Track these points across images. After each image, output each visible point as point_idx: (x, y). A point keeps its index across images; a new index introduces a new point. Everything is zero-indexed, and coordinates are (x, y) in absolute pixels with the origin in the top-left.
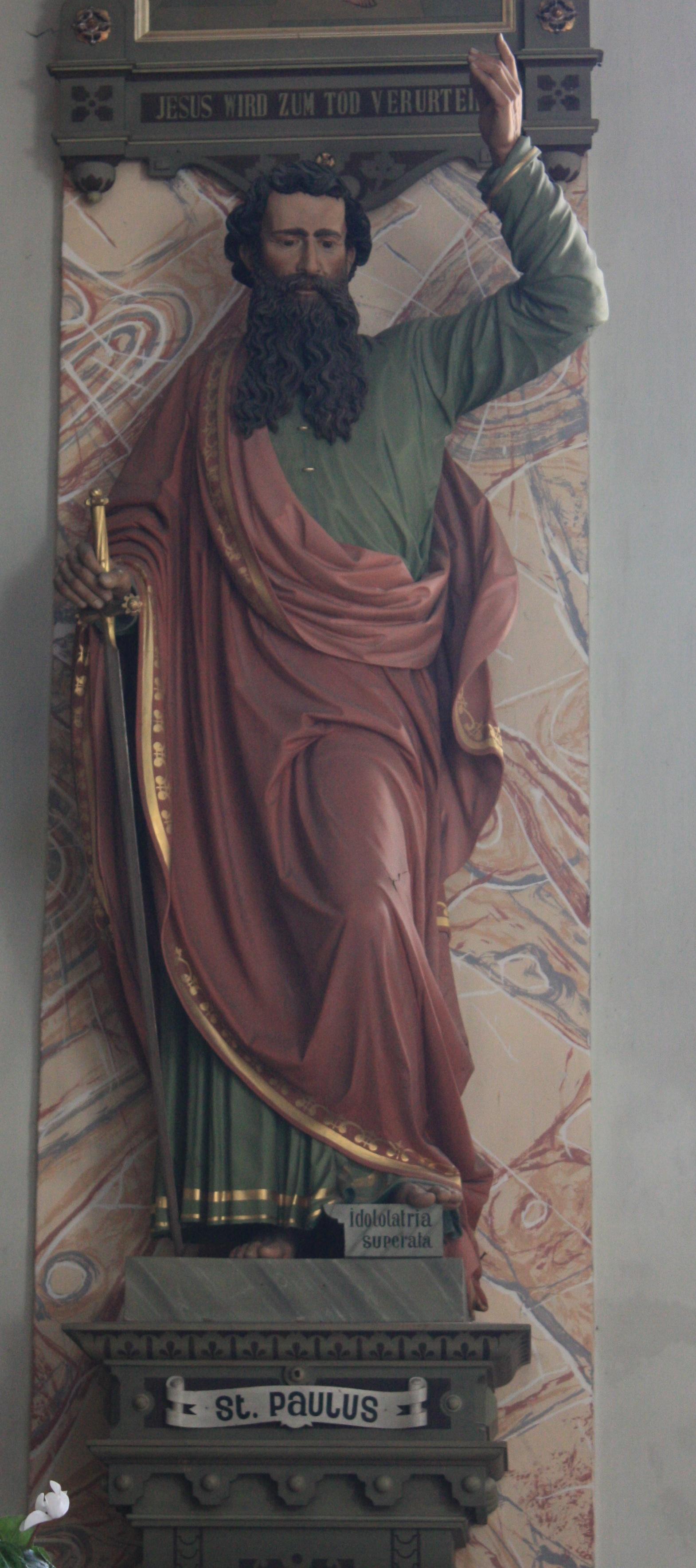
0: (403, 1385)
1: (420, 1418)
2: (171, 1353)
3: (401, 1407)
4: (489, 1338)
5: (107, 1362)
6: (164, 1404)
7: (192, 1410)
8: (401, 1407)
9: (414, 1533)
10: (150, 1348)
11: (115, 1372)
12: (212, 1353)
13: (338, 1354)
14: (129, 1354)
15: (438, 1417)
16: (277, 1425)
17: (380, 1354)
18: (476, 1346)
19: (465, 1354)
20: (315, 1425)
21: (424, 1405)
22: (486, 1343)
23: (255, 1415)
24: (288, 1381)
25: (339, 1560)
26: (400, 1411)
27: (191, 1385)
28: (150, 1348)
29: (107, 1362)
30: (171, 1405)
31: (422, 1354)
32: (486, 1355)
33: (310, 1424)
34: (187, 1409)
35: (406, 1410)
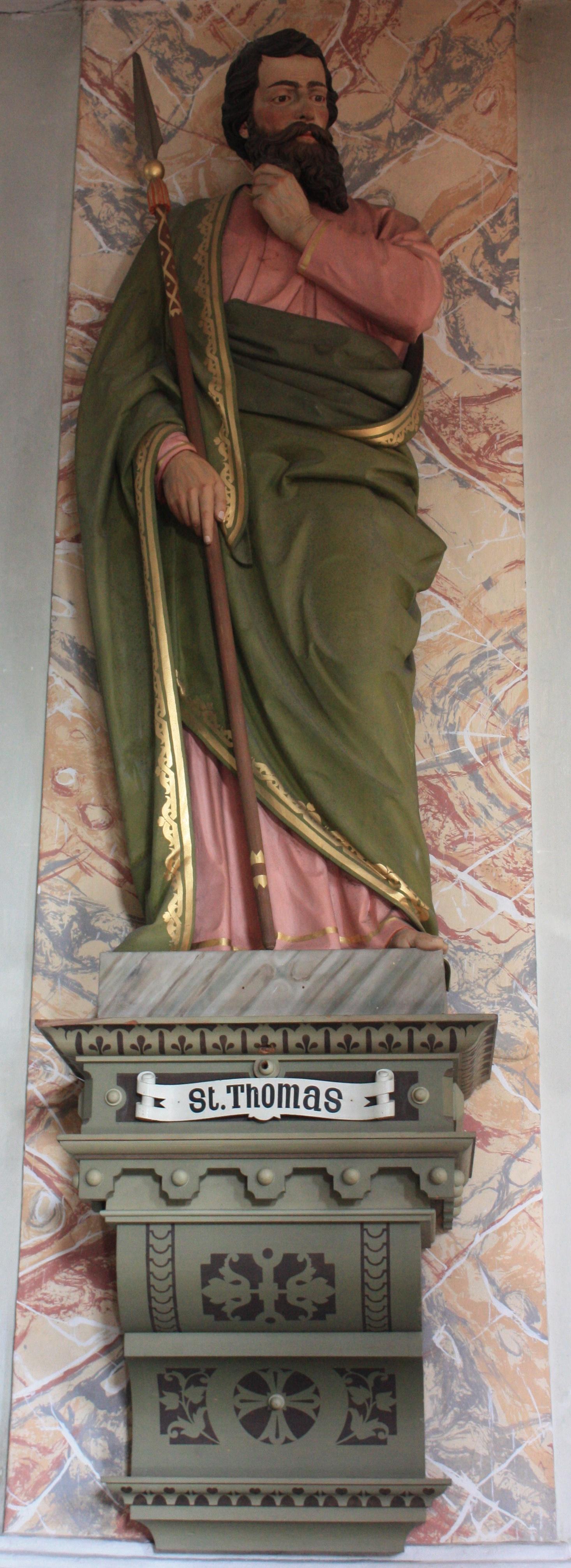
0: (370, 1078)
1: (387, 1109)
2: (141, 1048)
3: (368, 1098)
4: (456, 1029)
5: (79, 1059)
6: (135, 1097)
7: (162, 1103)
8: (368, 1098)
9: (385, 1227)
10: (203, 1043)
11: (87, 1068)
12: (182, 1048)
13: (306, 1047)
14: (100, 1048)
15: (406, 1109)
16: (245, 1117)
17: (348, 1046)
18: (443, 1037)
19: (431, 1046)
20: (285, 1117)
21: (392, 1096)
22: (452, 1032)
23: (223, 1107)
24: (257, 1074)
25: (310, 1255)
26: (368, 1102)
27: (162, 1079)
28: (203, 1043)
29: (79, 1059)
30: (139, 1098)
31: (389, 1046)
32: (453, 1048)
33: (279, 1117)
34: (158, 1102)
35: (373, 1101)
